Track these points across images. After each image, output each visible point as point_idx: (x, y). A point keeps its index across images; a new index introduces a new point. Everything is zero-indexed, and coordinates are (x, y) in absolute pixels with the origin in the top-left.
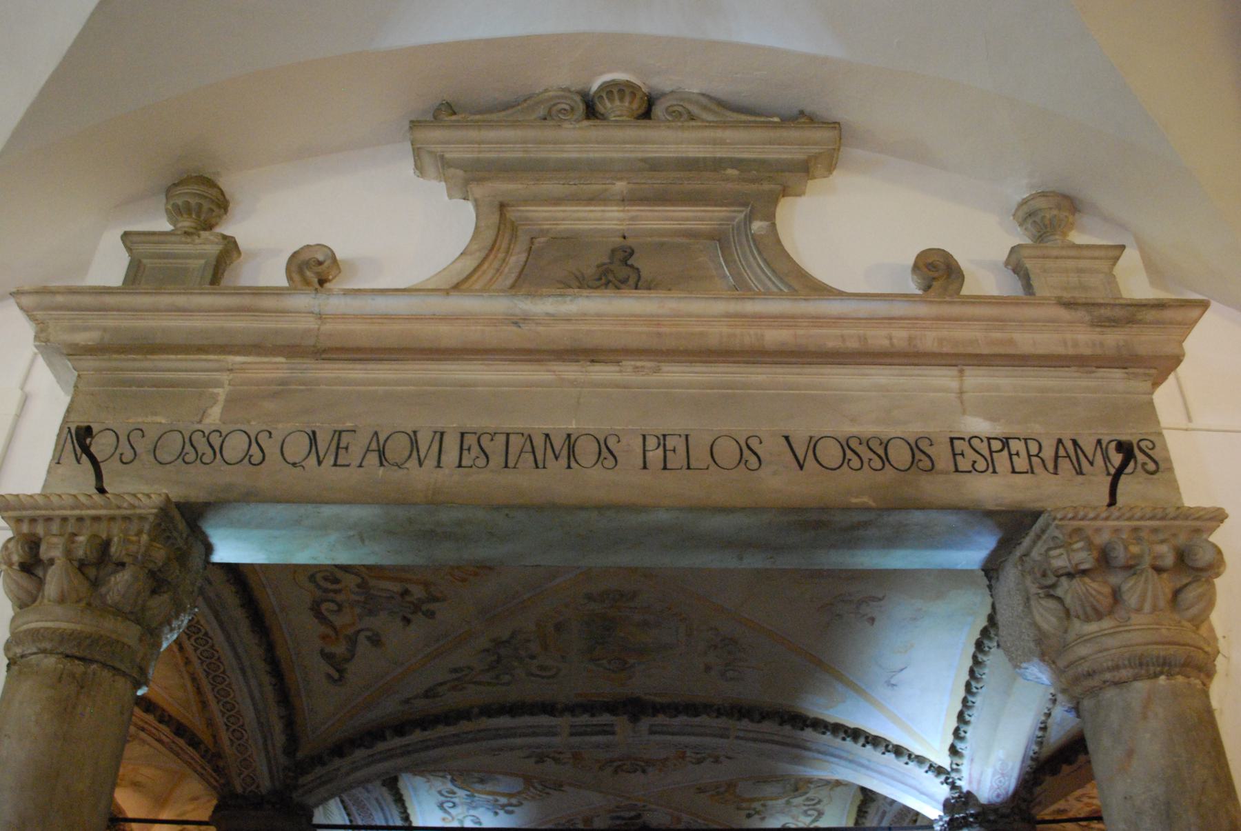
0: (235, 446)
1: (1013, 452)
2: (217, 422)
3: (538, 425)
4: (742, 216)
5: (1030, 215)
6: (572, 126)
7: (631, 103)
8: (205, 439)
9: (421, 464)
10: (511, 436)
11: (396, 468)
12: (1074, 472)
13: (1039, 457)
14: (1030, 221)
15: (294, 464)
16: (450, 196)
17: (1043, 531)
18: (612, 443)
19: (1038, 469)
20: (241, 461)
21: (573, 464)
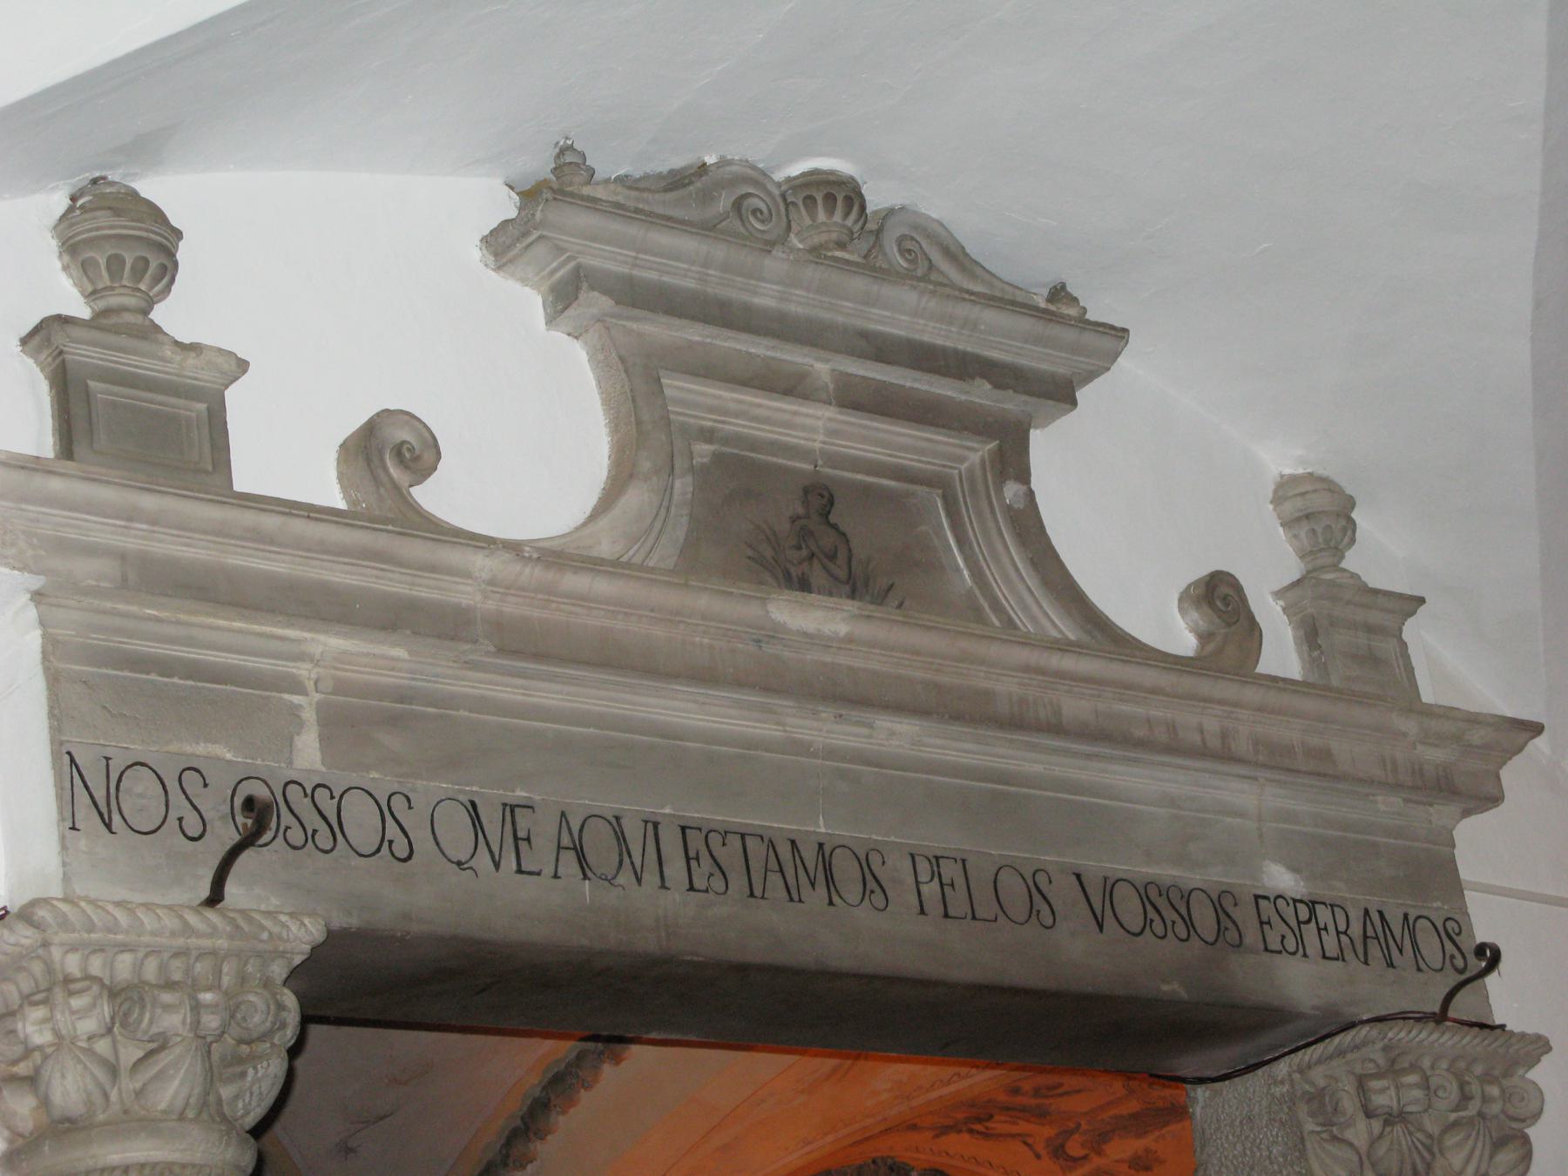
0: (361, 821)
1: (1322, 926)
2: (319, 766)
3: (780, 824)
4: (975, 458)
5: (1307, 517)
6: (784, 256)
7: (847, 215)
8: (308, 801)
9: (639, 880)
10: (750, 842)
11: (606, 883)
12: (1385, 965)
13: (1348, 936)
14: (1305, 527)
15: (459, 863)
16: (548, 330)
17: (1356, 1047)
18: (875, 860)
19: (1349, 955)
20: (378, 850)
21: (836, 899)
